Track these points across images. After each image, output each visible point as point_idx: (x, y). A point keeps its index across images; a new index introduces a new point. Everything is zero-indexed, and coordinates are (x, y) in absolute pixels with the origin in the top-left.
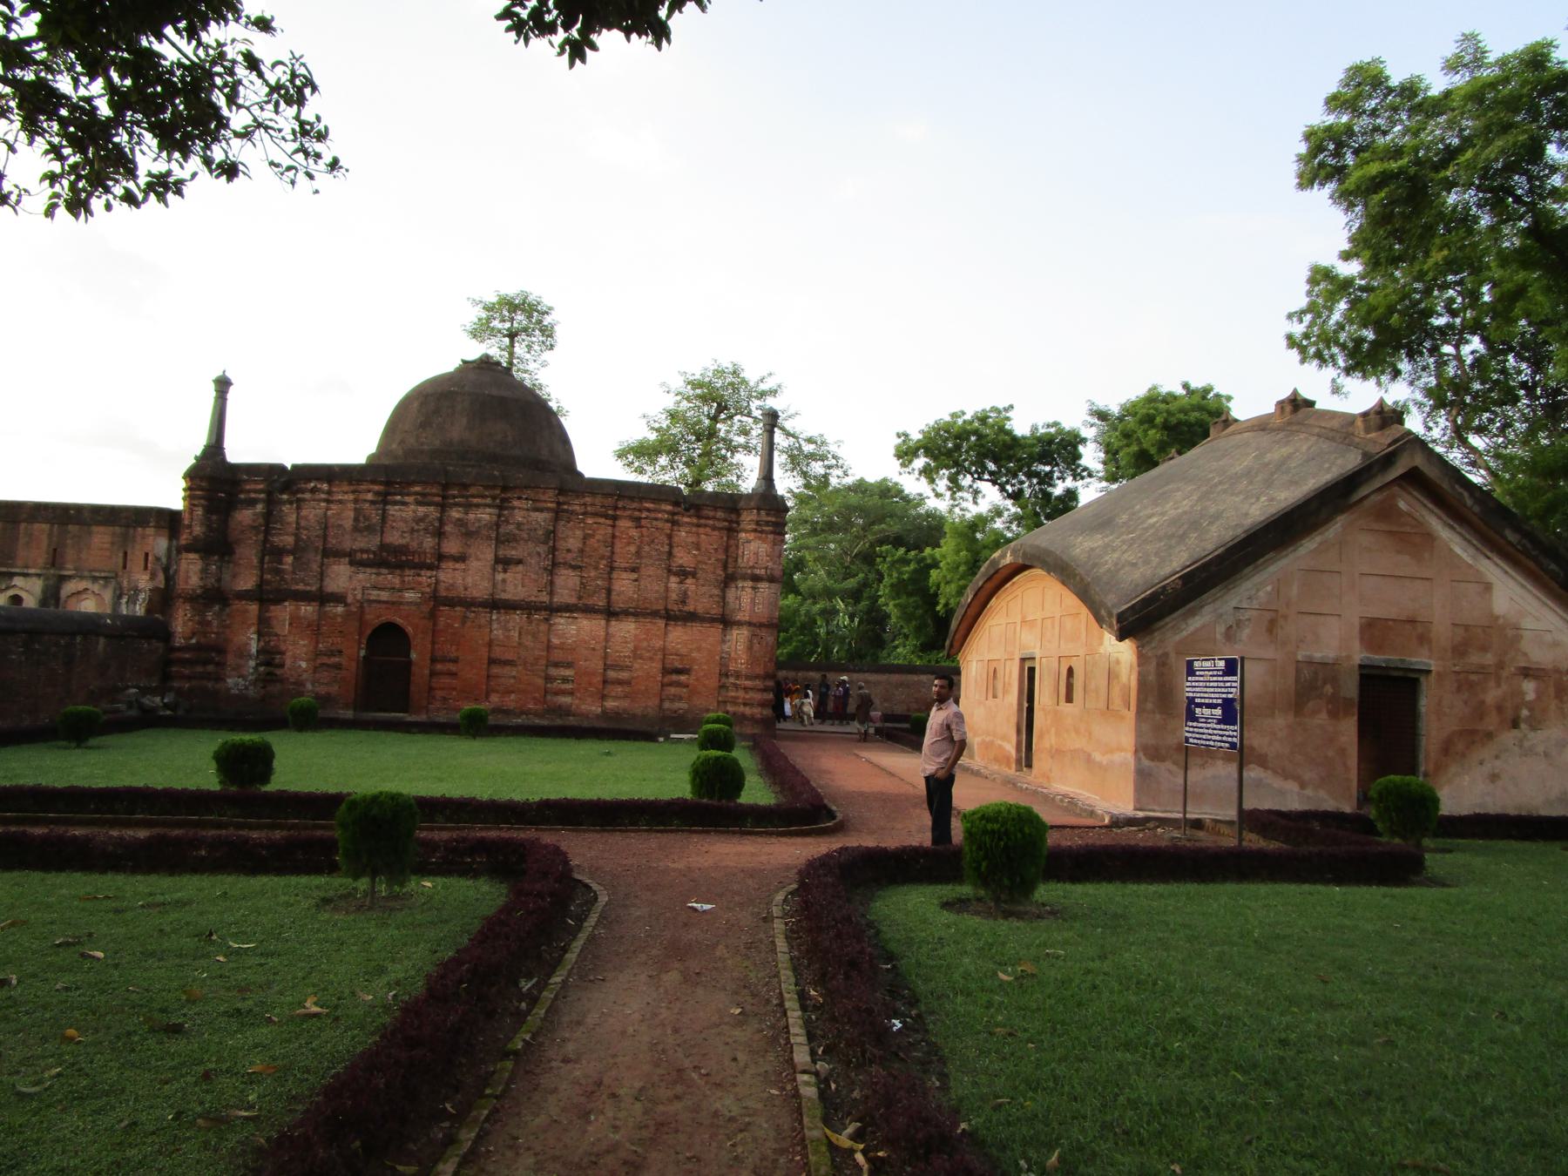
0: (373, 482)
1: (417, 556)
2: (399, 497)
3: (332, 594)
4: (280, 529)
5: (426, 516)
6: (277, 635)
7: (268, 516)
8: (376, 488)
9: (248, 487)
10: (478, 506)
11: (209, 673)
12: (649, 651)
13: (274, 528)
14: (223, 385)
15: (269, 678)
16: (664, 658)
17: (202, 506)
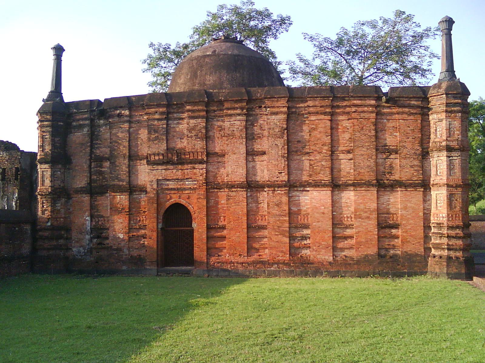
0: (159, 106)
1: (191, 155)
4: (99, 144)
6: (102, 217)
7: (93, 136)
8: (161, 110)
9: (78, 117)
10: (231, 115)
11: (61, 246)
12: (366, 212)
13: (97, 144)
14: (59, 50)
15: (100, 246)
16: (378, 217)
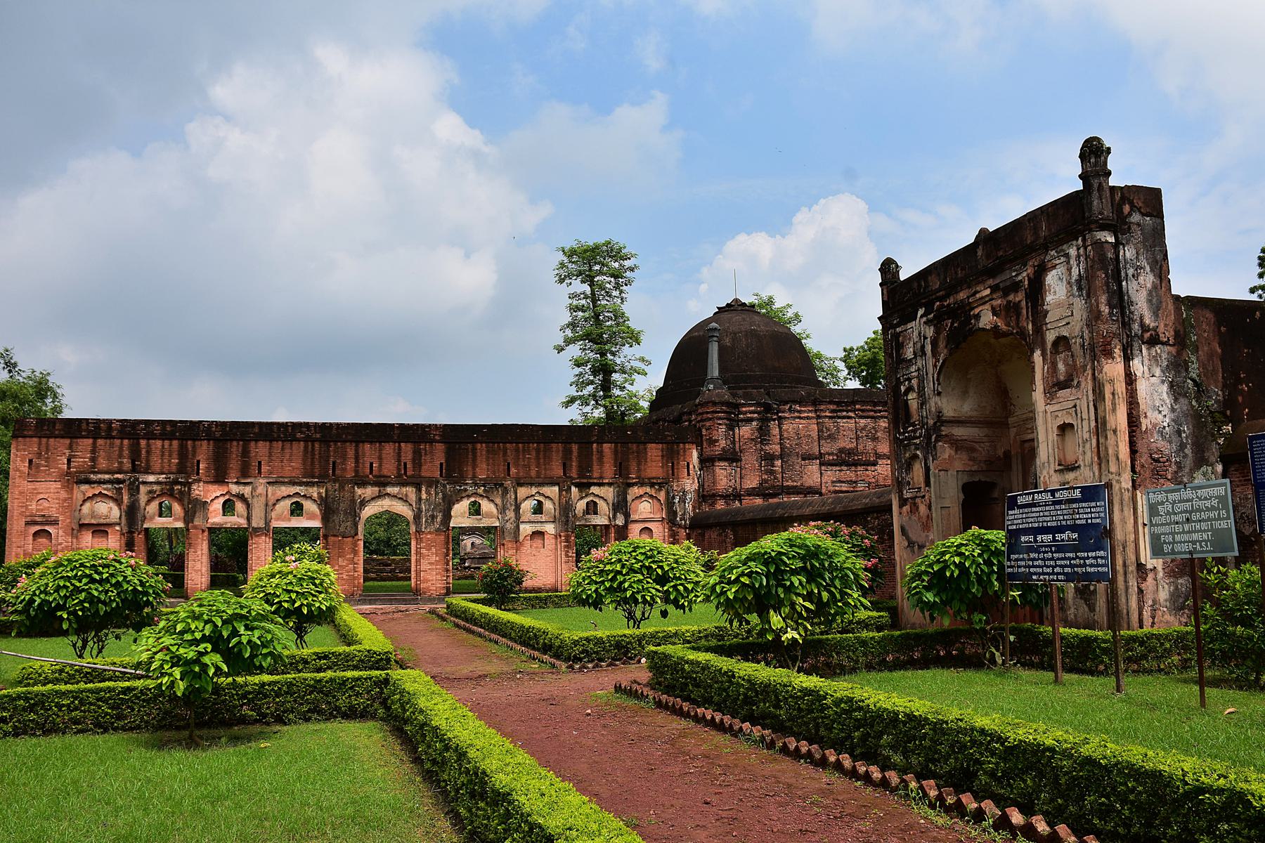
0: (831, 402)
2: (845, 413)
3: (810, 487)
5: (866, 426)
8: (832, 407)
13: (765, 440)
17: (726, 425)
